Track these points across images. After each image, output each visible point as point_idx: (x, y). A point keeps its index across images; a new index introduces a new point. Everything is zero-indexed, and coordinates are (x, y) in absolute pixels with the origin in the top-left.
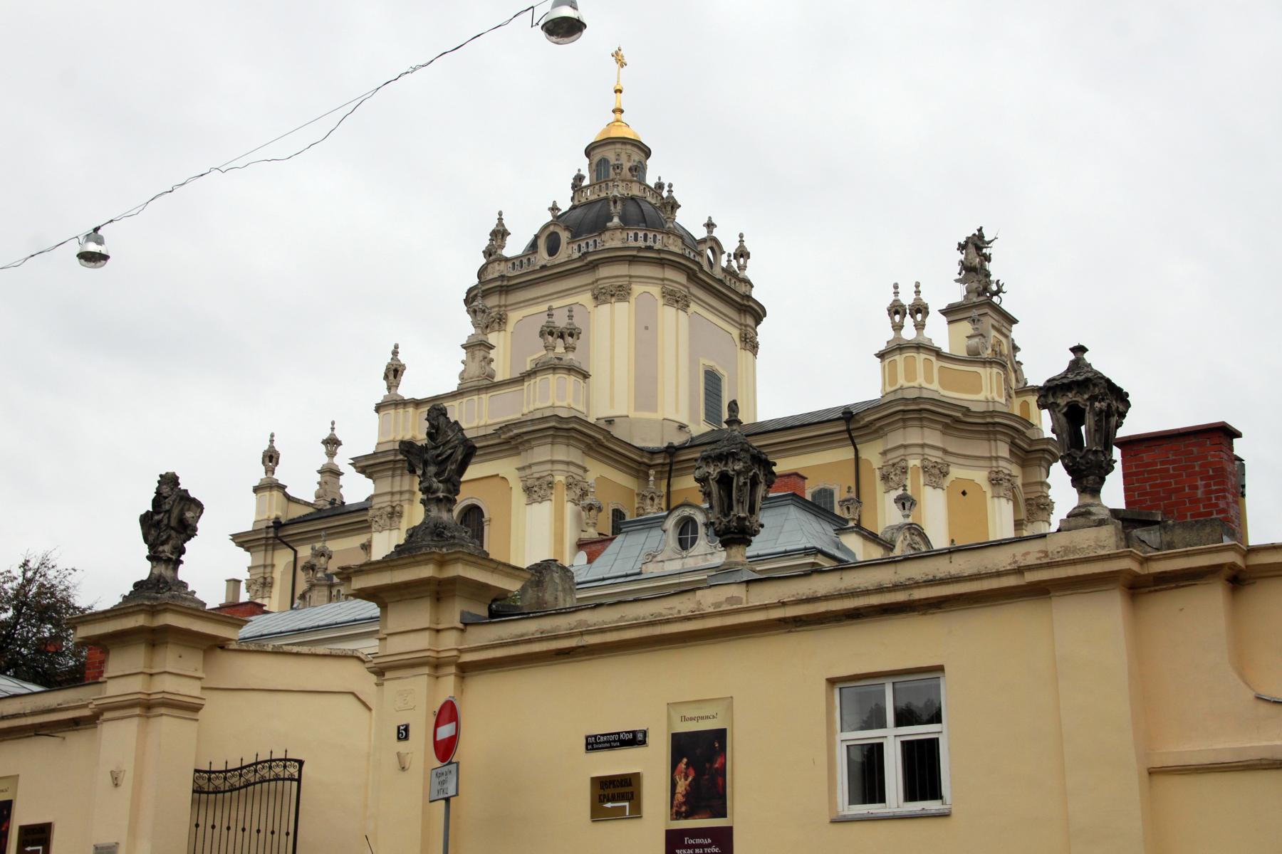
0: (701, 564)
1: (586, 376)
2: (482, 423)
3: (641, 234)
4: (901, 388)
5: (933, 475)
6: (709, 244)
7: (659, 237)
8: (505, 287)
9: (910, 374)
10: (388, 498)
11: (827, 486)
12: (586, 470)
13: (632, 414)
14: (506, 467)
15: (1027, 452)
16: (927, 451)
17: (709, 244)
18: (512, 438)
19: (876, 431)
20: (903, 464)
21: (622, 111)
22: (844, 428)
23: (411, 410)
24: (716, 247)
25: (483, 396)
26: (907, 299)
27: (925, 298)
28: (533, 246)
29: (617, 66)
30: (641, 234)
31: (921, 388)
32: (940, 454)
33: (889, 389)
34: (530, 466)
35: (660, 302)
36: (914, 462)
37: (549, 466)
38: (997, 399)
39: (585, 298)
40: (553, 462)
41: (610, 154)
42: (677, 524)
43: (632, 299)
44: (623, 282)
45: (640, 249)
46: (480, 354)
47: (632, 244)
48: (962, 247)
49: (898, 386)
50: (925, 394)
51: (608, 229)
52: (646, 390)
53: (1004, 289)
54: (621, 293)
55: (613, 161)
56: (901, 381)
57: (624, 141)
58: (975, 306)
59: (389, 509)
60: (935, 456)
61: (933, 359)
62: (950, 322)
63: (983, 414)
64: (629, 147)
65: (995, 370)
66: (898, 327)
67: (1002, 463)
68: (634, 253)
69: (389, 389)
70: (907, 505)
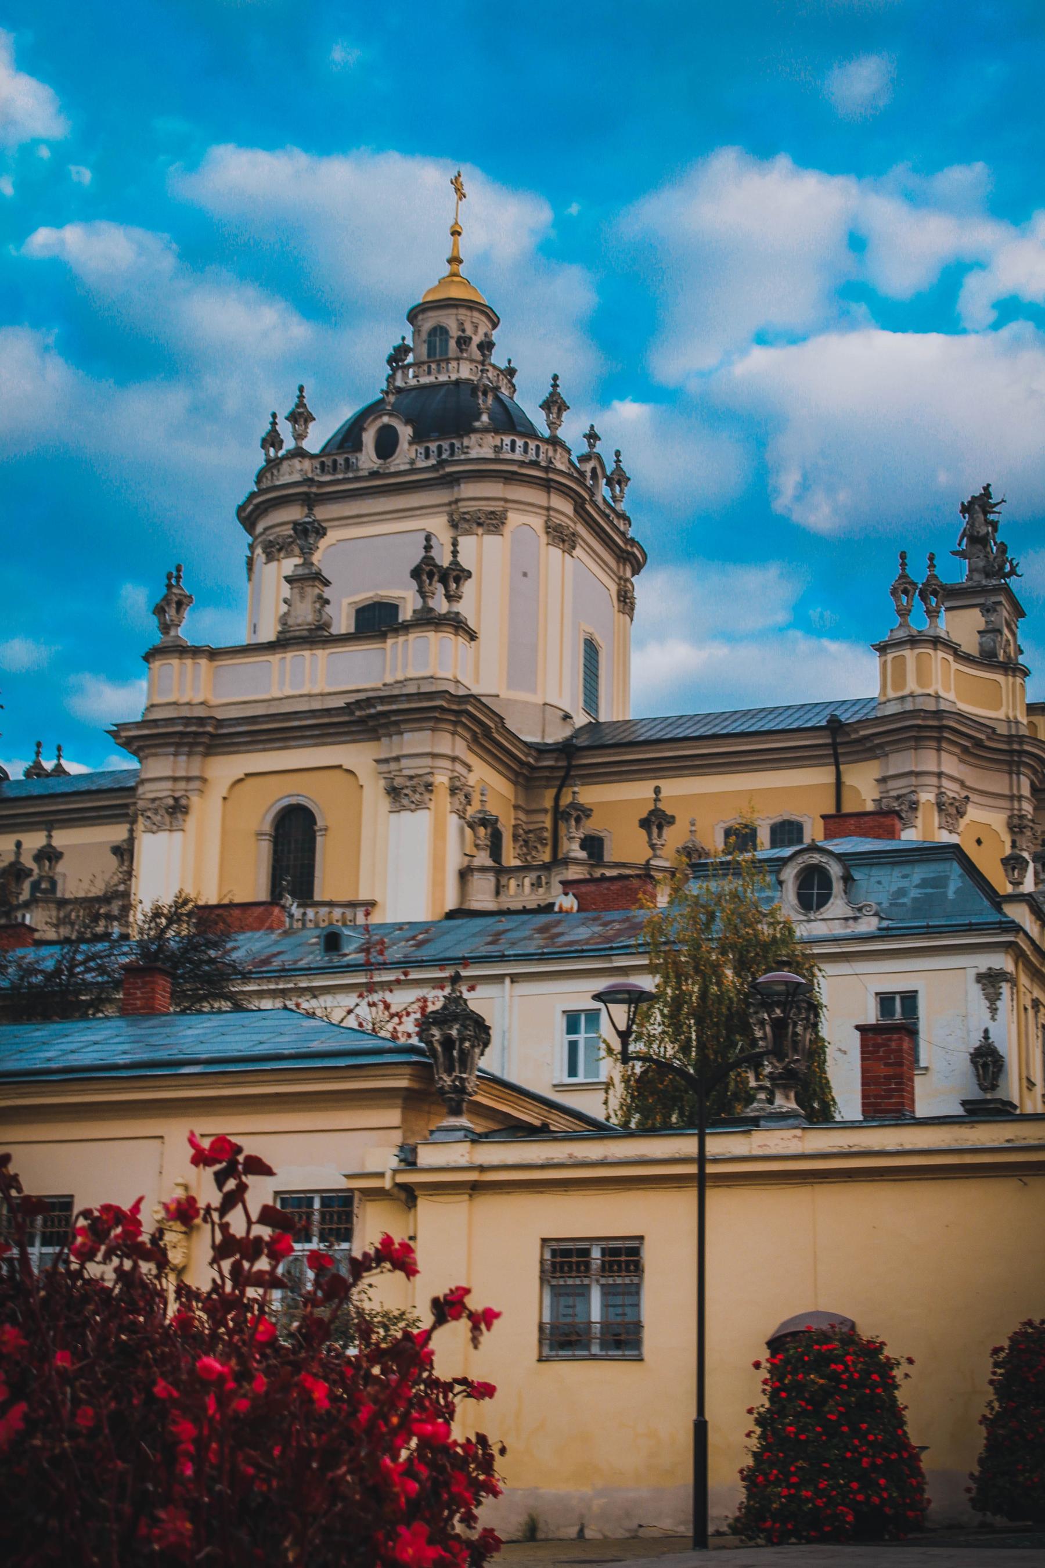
0: (838, 929)
2: (316, 690)
3: (520, 443)
4: (912, 695)
5: (949, 815)
8: (310, 498)
9: (922, 677)
10: (169, 785)
11: (794, 818)
12: (469, 768)
13: (503, 695)
14: (358, 756)
16: (945, 782)
18: (371, 716)
19: (871, 749)
20: (914, 798)
21: (461, 262)
22: (829, 741)
23: (203, 662)
25: (320, 653)
26: (919, 575)
28: (349, 438)
29: (456, 197)
31: (938, 697)
32: (956, 787)
33: (891, 694)
34: (397, 759)
35: (544, 539)
36: (927, 797)
37: (428, 761)
38: (1020, 719)
39: (438, 525)
40: (434, 756)
41: (450, 321)
42: (797, 876)
44: (496, 506)
45: (522, 464)
46: (312, 592)
48: (966, 509)
49: (906, 692)
50: (944, 706)
51: (475, 431)
52: (522, 663)
53: (1019, 571)
54: (492, 522)
55: (454, 332)
56: (912, 685)
57: (471, 305)
58: (984, 591)
59: (171, 802)
60: (952, 789)
61: (951, 658)
63: (1010, 738)
64: (476, 314)
66: (904, 613)
68: (514, 468)
69: (165, 628)
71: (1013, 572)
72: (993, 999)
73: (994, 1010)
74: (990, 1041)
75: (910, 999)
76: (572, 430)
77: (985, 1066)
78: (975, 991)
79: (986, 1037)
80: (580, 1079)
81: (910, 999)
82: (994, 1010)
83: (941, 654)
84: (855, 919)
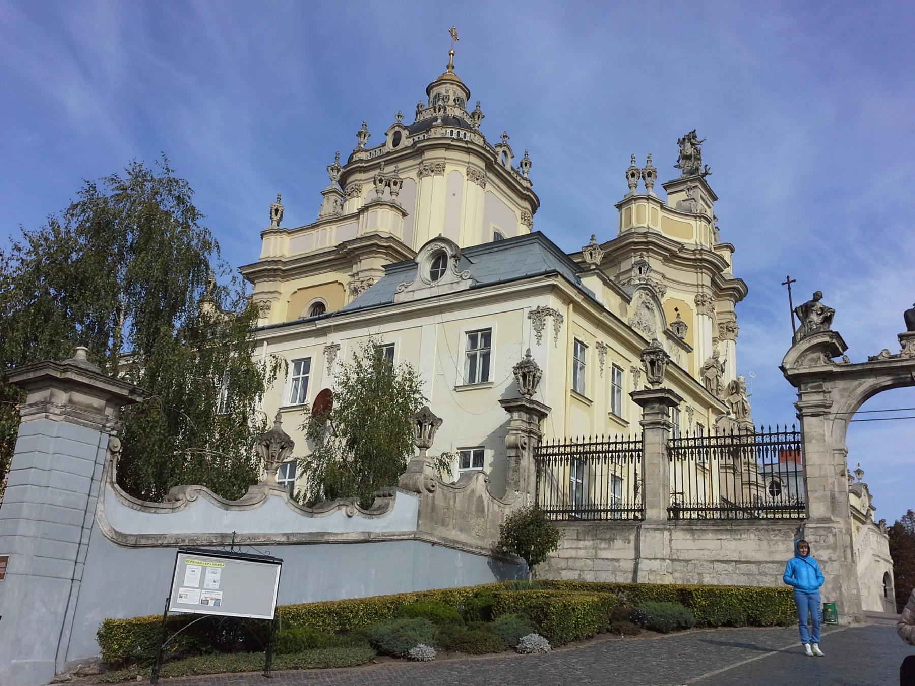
1: (404, 215)
3: (455, 131)
7: (468, 134)
18: (347, 253)
25: (334, 227)
26: (641, 165)
27: (654, 165)
30: (455, 131)
32: (660, 277)
34: (358, 274)
35: (466, 178)
43: (446, 173)
44: (440, 161)
47: (448, 135)
48: (681, 142)
53: (710, 172)
54: (439, 169)
61: (659, 209)
63: (694, 252)
64: (455, 87)
65: (704, 223)
67: (706, 290)
68: (449, 142)
78: (528, 323)
79: (528, 356)
80: (297, 404)
81: (487, 334)
83: (651, 206)
84: (458, 282)
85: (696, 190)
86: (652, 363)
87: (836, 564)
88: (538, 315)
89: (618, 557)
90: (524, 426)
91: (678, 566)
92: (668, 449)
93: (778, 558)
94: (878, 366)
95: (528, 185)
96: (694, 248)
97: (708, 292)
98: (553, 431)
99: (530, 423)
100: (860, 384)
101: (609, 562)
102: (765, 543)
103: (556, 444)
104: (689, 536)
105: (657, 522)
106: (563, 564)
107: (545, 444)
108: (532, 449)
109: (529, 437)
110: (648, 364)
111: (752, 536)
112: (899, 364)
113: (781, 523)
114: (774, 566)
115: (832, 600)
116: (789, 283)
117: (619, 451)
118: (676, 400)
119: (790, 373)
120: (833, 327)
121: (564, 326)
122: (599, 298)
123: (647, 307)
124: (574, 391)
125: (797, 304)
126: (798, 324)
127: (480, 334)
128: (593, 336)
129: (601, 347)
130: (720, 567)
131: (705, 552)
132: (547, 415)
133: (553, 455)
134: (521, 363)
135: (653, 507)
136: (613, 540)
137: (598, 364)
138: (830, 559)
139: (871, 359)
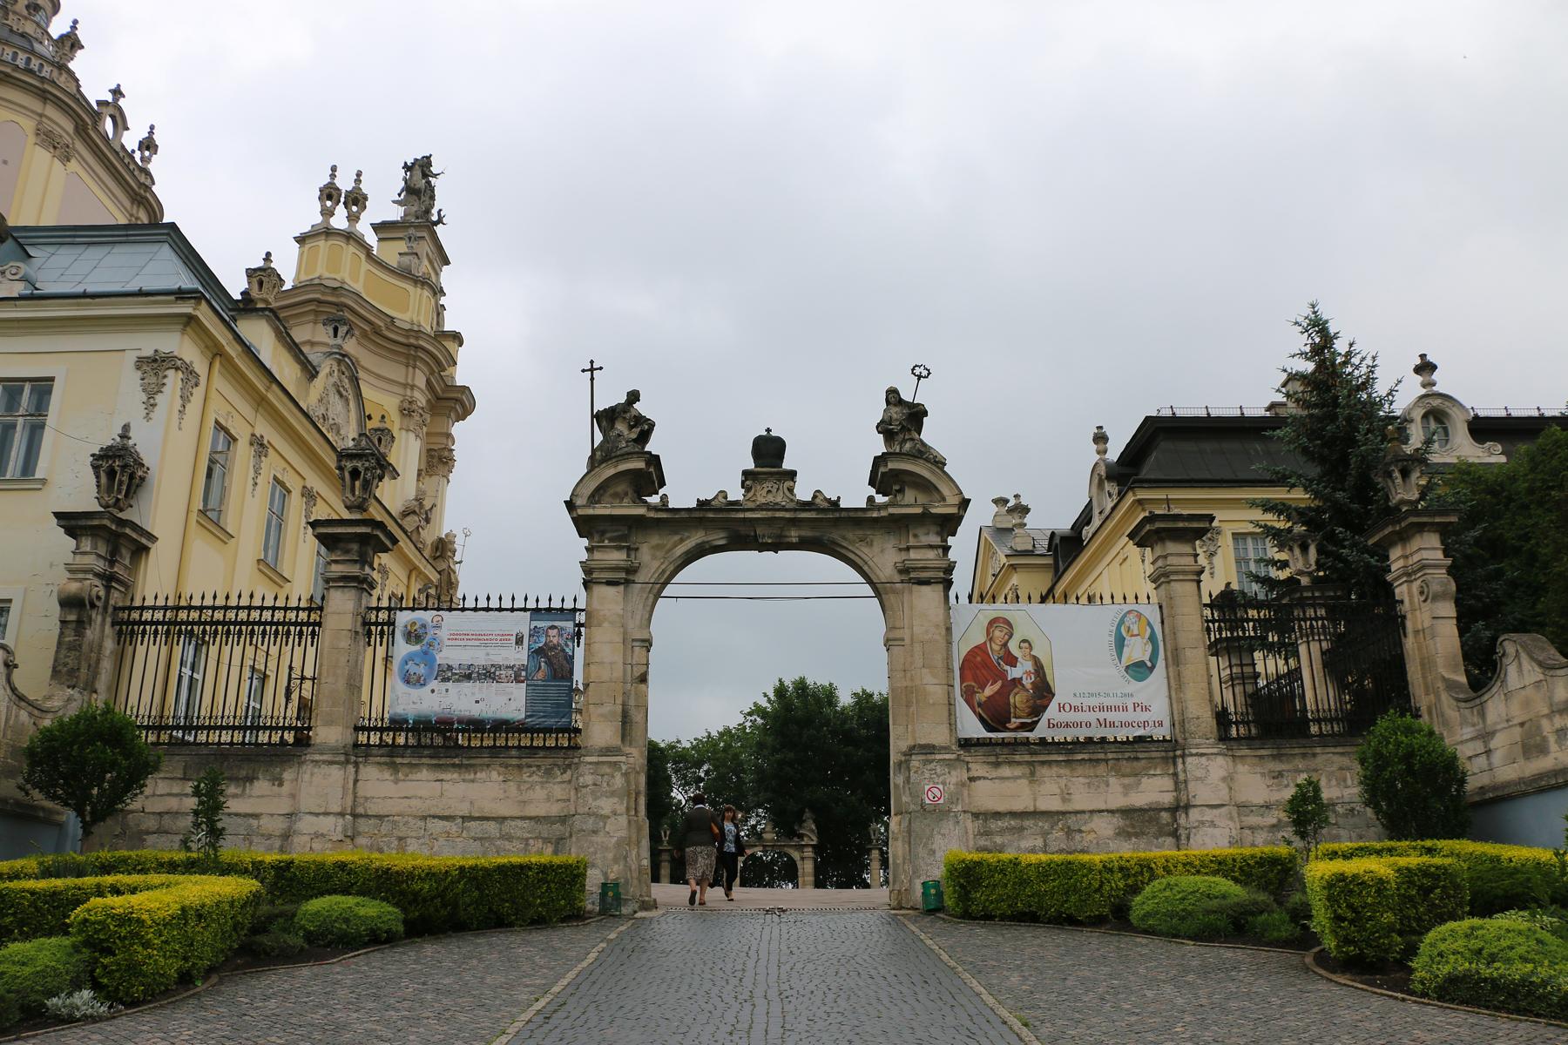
6: (111, 110)
15: (439, 399)
17: (111, 110)
24: (120, 122)
26: (345, 184)
27: (364, 188)
33: (304, 278)
48: (407, 167)
56: (321, 271)
61: (363, 257)
62: (380, 240)
63: (408, 333)
65: (427, 293)
66: (328, 213)
70: (343, 330)
71: (440, 221)
72: (152, 394)
73: (150, 406)
74: (131, 442)
75: (43, 387)
76: (93, 76)
77: (111, 474)
79: (124, 436)
82: (150, 406)
85: (422, 242)
86: (355, 474)
87: (623, 820)
88: (155, 364)
89: (258, 811)
90: (100, 566)
91: (363, 825)
92: (366, 623)
93: (532, 811)
94: (711, 515)
95: (148, 182)
96: (407, 327)
97: (421, 399)
98: (155, 582)
99: (112, 563)
100: (682, 540)
101: (239, 820)
102: (512, 787)
103: (161, 602)
104: (387, 775)
105: (334, 750)
106: (151, 823)
107: (137, 603)
108: (110, 610)
109: (108, 588)
110: (347, 475)
111: (494, 775)
112: (741, 515)
113: (541, 754)
114: (526, 824)
115: (612, 876)
116: (592, 370)
117: (278, 623)
118: (388, 543)
119: (580, 512)
120: (652, 447)
121: (198, 393)
122: (266, 358)
123: (341, 395)
124: (203, 512)
125: (600, 406)
126: (599, 437)
127: (27, 387)
128: (245, 421)
129: (260, 445)
130: (437, 826)
131: (413, 802)
132: (147, 549)
133: (152, 623)
134: (110, 448)
135: (329, 723)
136: (251, 779)
137: (252, 473)
138: (615, 813)
139: (703, 504)
